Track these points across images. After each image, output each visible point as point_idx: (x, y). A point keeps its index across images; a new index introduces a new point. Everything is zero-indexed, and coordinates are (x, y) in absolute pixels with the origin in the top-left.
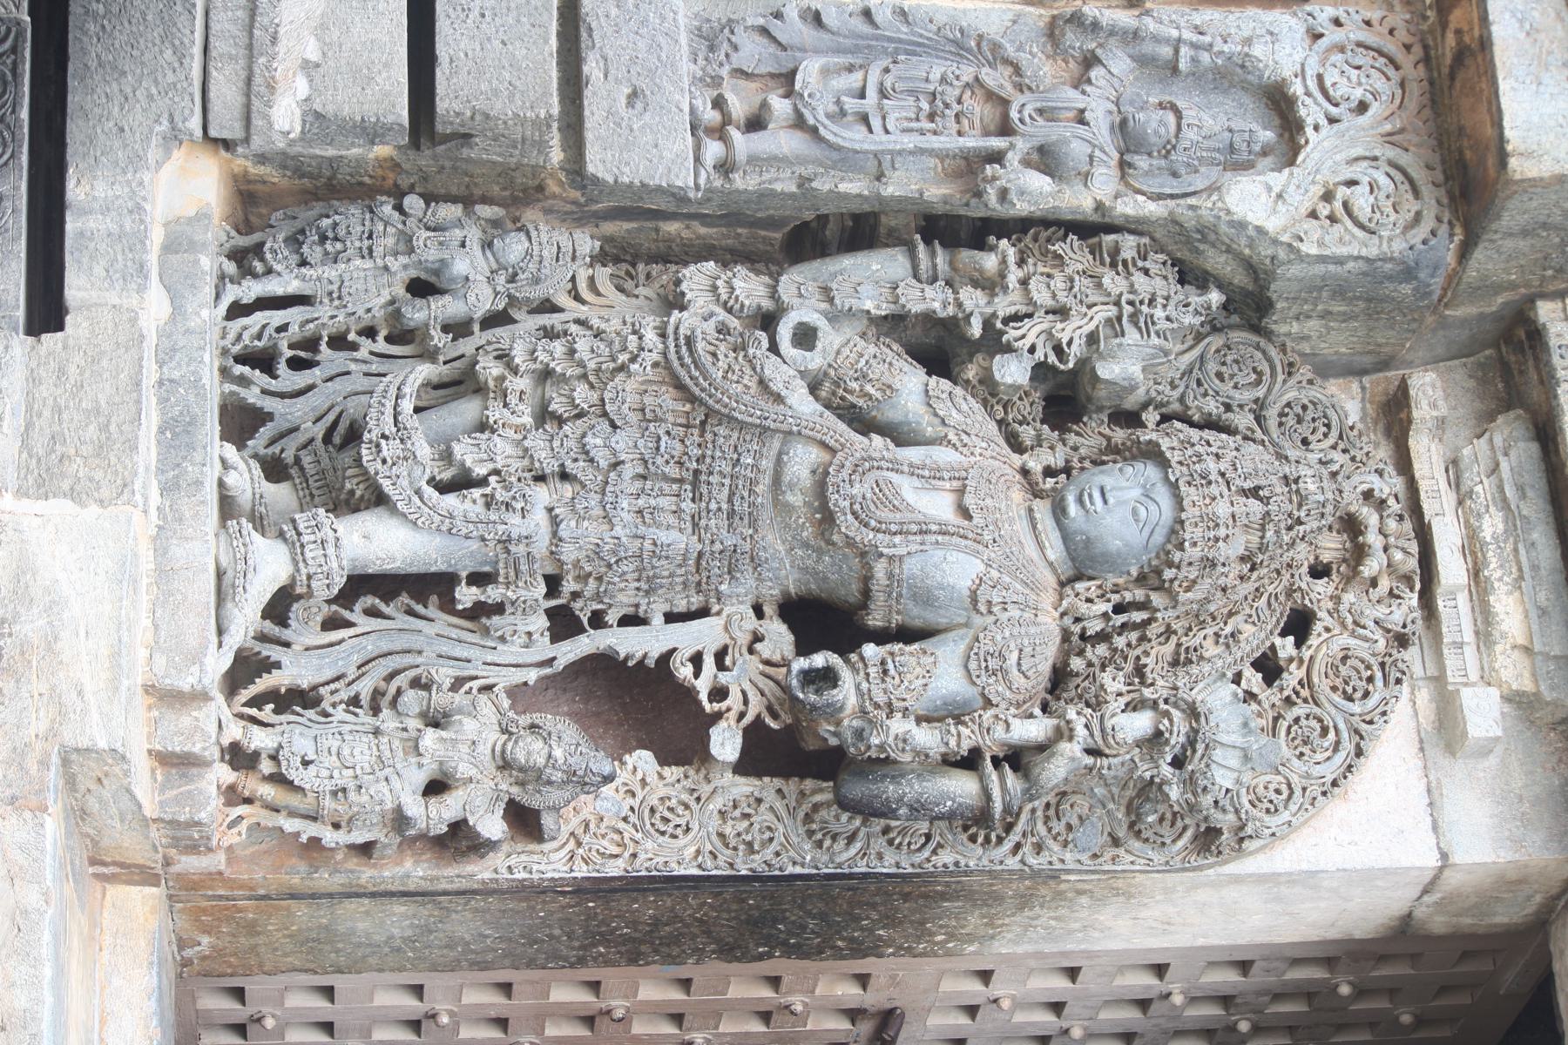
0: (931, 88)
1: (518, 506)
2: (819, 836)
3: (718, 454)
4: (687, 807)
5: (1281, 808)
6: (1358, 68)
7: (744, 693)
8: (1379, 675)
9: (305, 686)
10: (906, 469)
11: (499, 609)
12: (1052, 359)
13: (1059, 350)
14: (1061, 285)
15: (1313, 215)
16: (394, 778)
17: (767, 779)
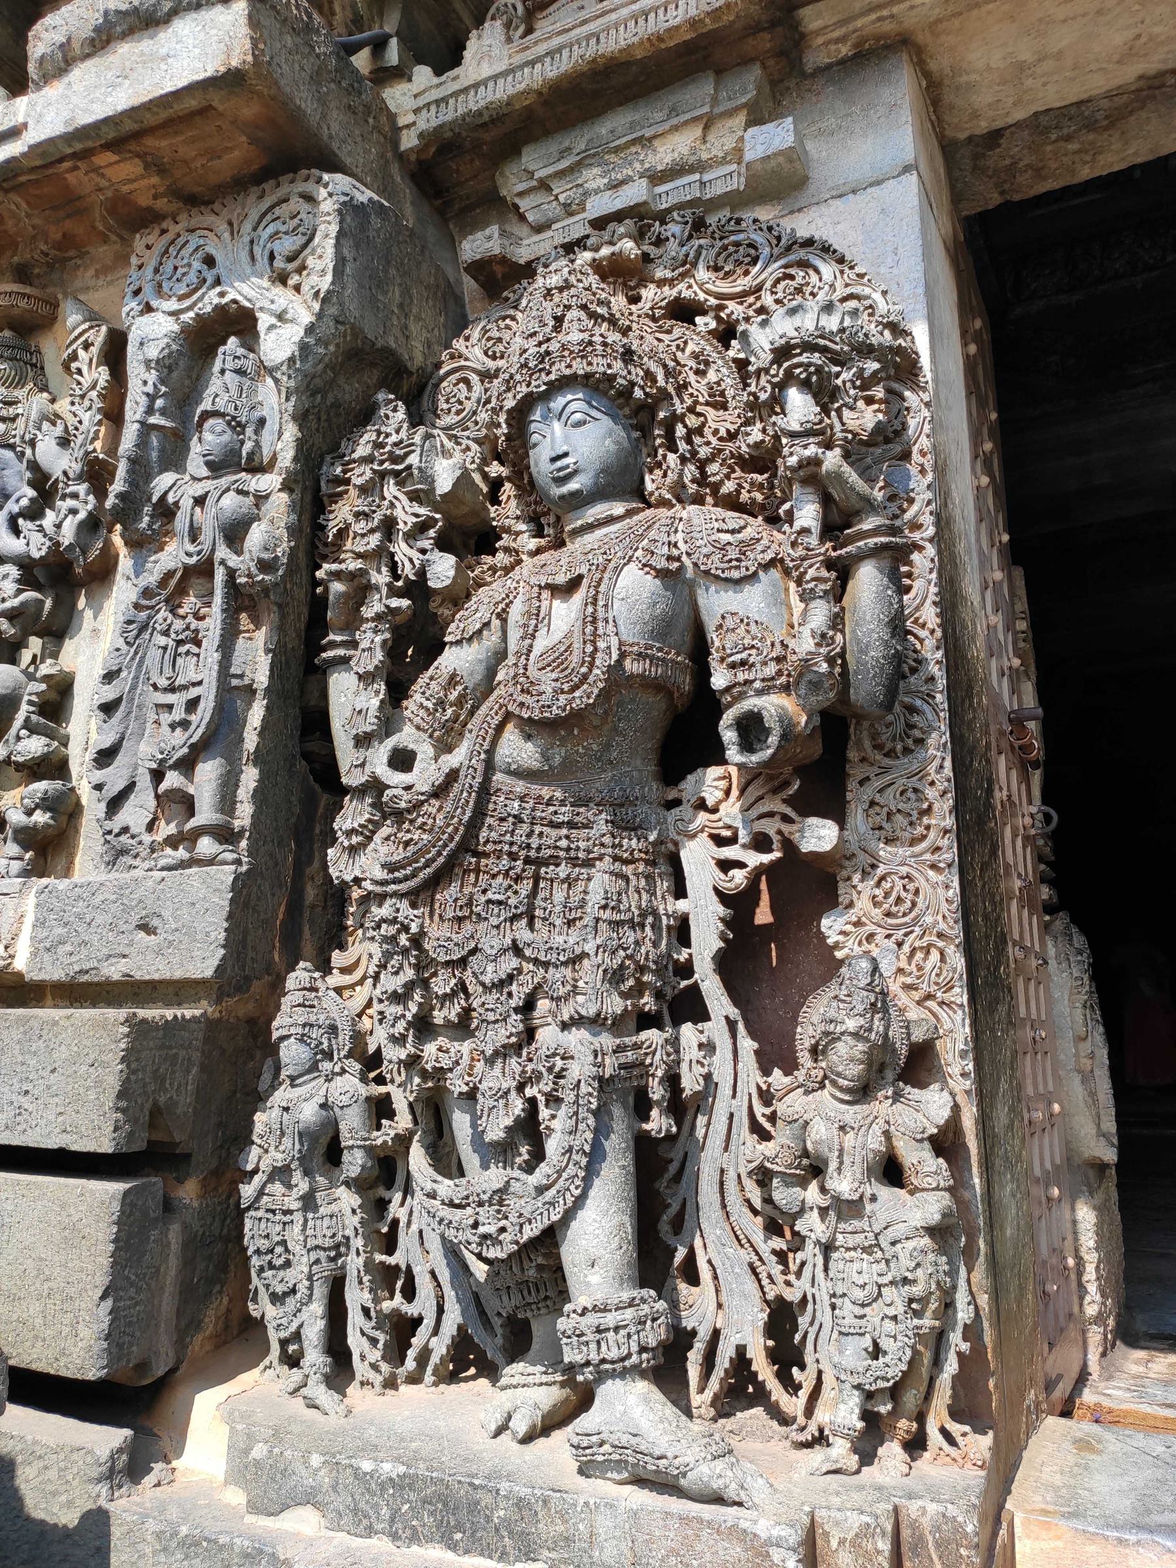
0: (171, 643)
1: (559, 1063)
2: (910, 742)
3: (508, 837)
4: (883, 878)
5: (867, 303)
6: (176, 268)
7: (760, 817)
8: (732, 238)
9: (764, 1316)
10: (528, 641)
11: (673, 1080)
12: (432, 533)
13: (422, 528)
14: (363, 524)
15: (297, 288)
16: (891, 1234)
17: (849, 796)
